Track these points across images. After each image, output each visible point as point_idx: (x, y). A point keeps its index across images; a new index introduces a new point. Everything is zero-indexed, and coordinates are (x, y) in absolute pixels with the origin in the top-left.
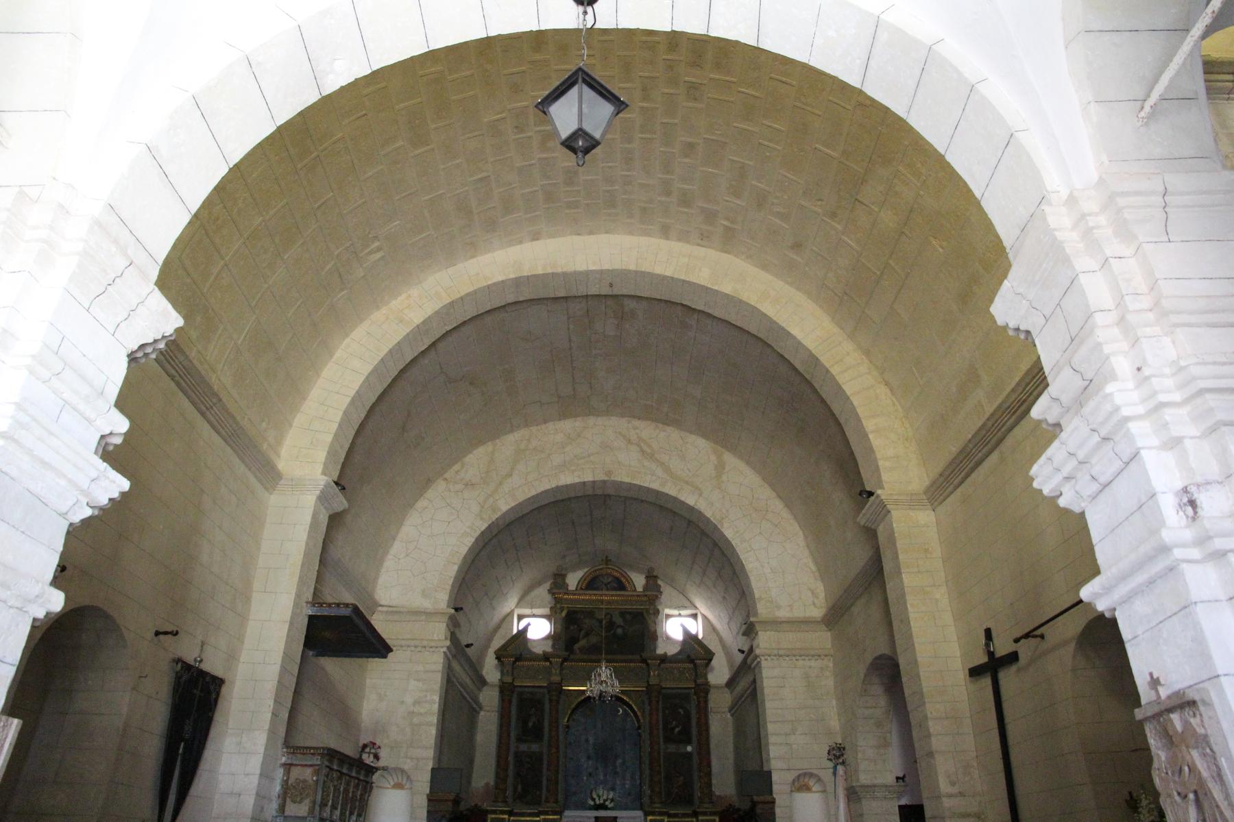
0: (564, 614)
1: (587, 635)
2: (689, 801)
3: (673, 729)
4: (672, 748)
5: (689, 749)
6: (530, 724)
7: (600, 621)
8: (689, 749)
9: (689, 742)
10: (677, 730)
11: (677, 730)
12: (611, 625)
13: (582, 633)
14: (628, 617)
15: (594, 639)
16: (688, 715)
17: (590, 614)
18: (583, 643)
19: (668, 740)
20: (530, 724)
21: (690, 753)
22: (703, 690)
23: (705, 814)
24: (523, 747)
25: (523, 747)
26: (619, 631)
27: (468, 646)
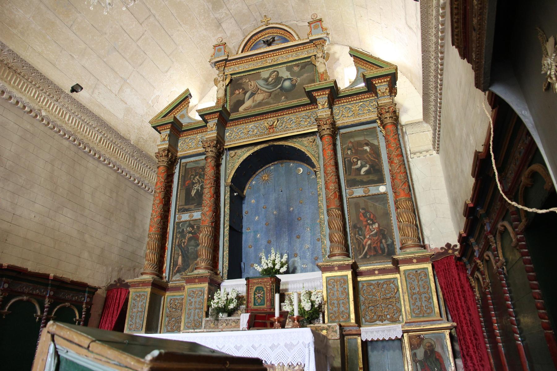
0: (228, 81)
1: (253, 94)
2: (389, 253)
3: (359, 169)
4: (359, 192)
5: (382, 189)
6: (193, 193)
7: (266, 80)
8: (382, 189)
9: (381, 181)
10: (364, 169)
11: (364, 169)
12: (278, 79)
13: (248, 95)
14: (296, 69)
15: (259, 97)
16: (376, 151)
17: (254, 74)
18: (248, 103)
19: (352, 183)
20: (193, 193)
21: (384, 194)
22: (391, 119)
23: (408, 261)
24: (185, 217)
25: (185, 217)
26: (287, 84)
27: (75, 89)
